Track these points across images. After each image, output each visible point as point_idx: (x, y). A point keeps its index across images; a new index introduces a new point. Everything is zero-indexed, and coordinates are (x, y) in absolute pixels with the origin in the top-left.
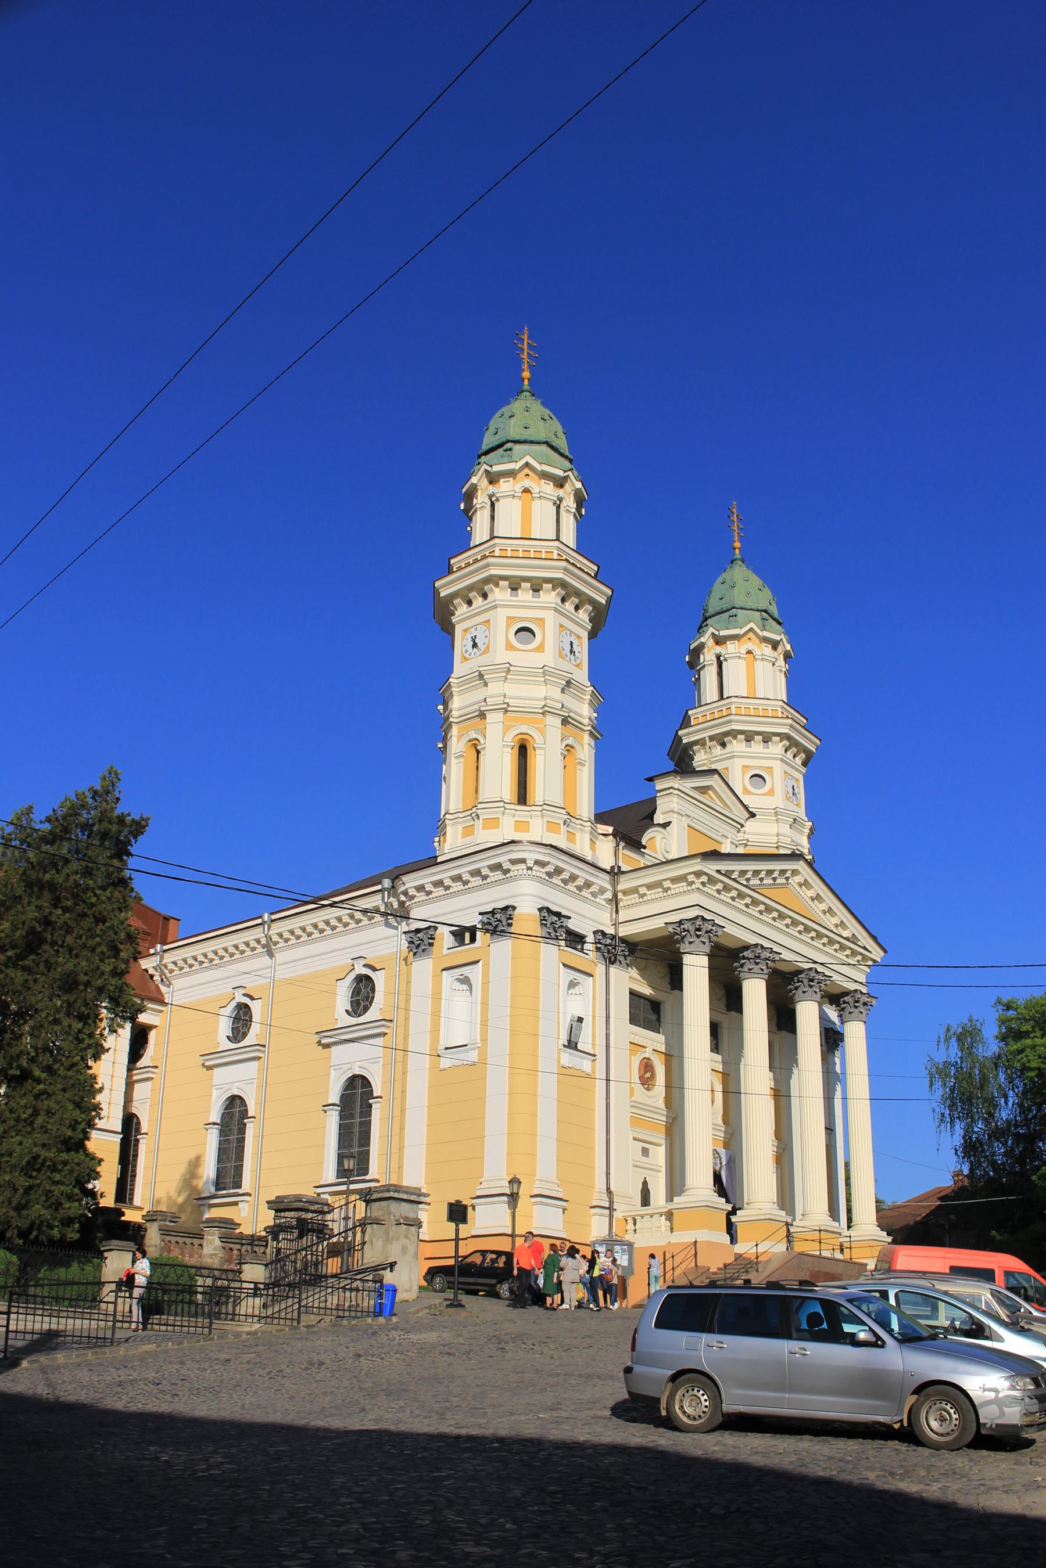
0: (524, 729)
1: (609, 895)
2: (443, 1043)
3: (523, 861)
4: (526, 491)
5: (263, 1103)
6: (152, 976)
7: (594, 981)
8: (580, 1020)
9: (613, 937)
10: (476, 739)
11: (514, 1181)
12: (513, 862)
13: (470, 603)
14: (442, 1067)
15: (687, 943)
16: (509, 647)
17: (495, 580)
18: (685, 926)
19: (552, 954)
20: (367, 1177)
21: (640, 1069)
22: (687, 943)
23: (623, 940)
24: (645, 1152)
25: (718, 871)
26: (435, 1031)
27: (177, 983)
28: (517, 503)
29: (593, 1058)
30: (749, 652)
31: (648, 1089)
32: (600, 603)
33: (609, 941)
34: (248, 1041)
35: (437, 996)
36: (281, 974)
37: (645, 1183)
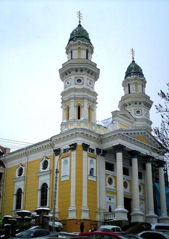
1: (99, 140)
3: (78, 133)
4: (80, 48)
5: (26, 189)
8: (93, 169)
13: (67, 75)
14: (62, 180)
16: (76, 84)
17: (72, 69)
19: (85, 154)
24: (110, 199)
27: (9, 163)
28: (77, 51)
30: (136, 82)
36: (29, 161)
37: (110, 206)
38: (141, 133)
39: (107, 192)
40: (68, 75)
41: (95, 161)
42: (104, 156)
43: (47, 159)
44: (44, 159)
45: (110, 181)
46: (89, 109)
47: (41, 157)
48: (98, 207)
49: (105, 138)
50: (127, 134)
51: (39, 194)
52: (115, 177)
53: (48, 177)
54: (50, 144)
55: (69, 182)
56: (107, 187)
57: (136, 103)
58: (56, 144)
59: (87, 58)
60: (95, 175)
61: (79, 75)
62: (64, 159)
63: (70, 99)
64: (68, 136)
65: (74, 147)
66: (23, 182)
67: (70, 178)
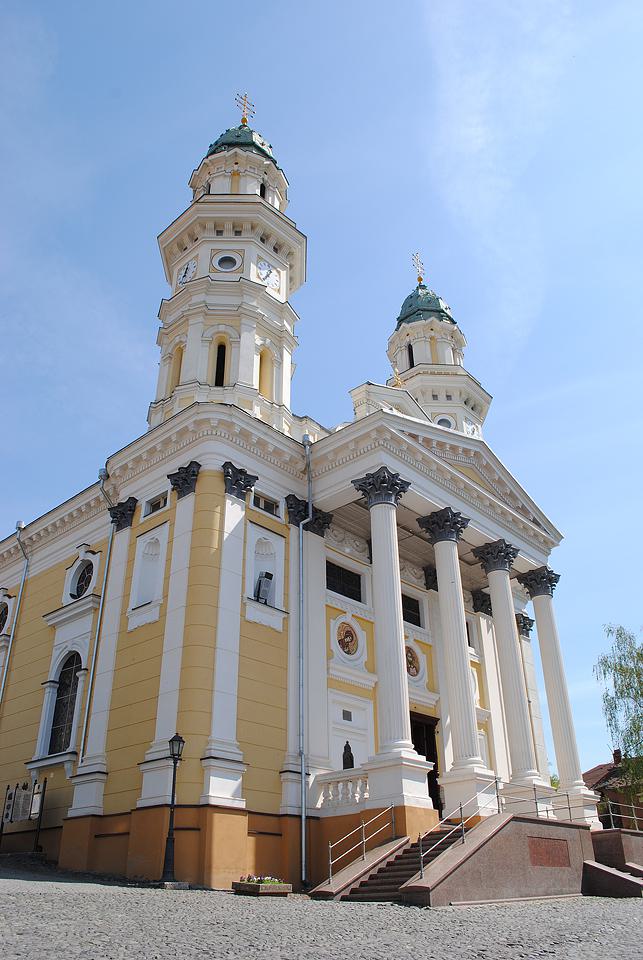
0: (222, 328)
1: (301, 466)
3: (208, 420)
7: (287, 543)
8: (269, 576)
11: (177, 739)
12: (198, 423)
20: (68, 750)
21: (339, 634)
23: (316, 511)
24: (347, 716)
26: (126, 596)
29: (285, 615)
31: (348, 653)
33: (302, 508)
35: (130, 561)
37: (347, 748)
38: (466, 451)
39: (333, 683)
40: (190, 246)
41: (278, 544)
43: (90, 557)
44: (81, 558)
45: (347, 641)
47: (71, 552)
48: (292, 749)
50: (414, 437)
51: (49, 698)
52: (369, 625)
53: (86, 624)
54: (106, 494)
55: (156, 629)
57: (435, 397)
59: (263, 194)
60: (278, 602)
61: (228, 245)
63: (184, 319)
64: (167, 442)
65: (185, 480)
67: (163, 615)
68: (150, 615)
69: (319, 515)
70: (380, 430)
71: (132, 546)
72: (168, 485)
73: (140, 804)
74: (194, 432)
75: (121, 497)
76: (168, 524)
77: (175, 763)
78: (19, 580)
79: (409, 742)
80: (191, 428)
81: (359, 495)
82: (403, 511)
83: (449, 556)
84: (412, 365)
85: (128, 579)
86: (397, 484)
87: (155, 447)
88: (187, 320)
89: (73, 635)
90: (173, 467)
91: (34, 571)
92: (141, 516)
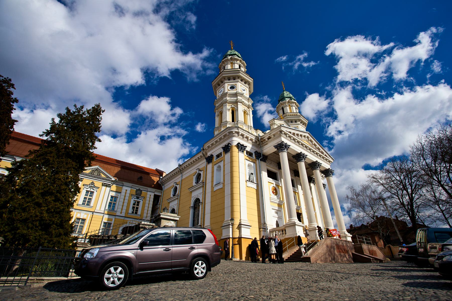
0: (233, 106)
1: (258, 143)
2: (215, 183)
3: (232, 132)
6: (161, 184)
7: (256, 165)
8: (252, 174)
9: (260, 154)
10: (221, 111)
14: (214, 190)
15: (280, 150)
17: (224, 78)
18: (279, 145)
20: (199, 225)
21: (272, 190)
22: (280, 150)
23: (263, 155)
25: (287, 131)
26: (212, 181)
27: (165, 185)
32: (250, 82)
33: (259, 155)
34: (177, 194)
35: (213, 172)
36: (184, 178)
38: (304, 136)
40: (221, 84)
42: (265, 162)
44: (197, 172)
46: (245, 112)
47: (194, 171)
49: (265, 140)
51: (191, 211)
53: (201, 190)
54: (203, 154)
56: (272, 197)
58: (209, 151)
59: (240, 68)
62: (217, 165)
66: (176, 202)
67: (224, 186)
68: (220, 186)
69: (264, 156)
70: (281, 131)
71: (213, 168)
72: (222, 150)
73: (222, 238)
74: (228, 135)
75: (208, 155)
76: (223, 161)
77: (232, 226)
78: (180, 180)
79: (297, 218)
80: (227, 134)
81: (276, 150)
82: (289, 154)
83: (302, 166)
84: (284, 113)
85: (213, 177)
86: (287, 146)
87: (217, 140)
88: (223, 105)
89: (198, 194)
90: (223, 145)
91: (184, 177)
92: (215, 159)
